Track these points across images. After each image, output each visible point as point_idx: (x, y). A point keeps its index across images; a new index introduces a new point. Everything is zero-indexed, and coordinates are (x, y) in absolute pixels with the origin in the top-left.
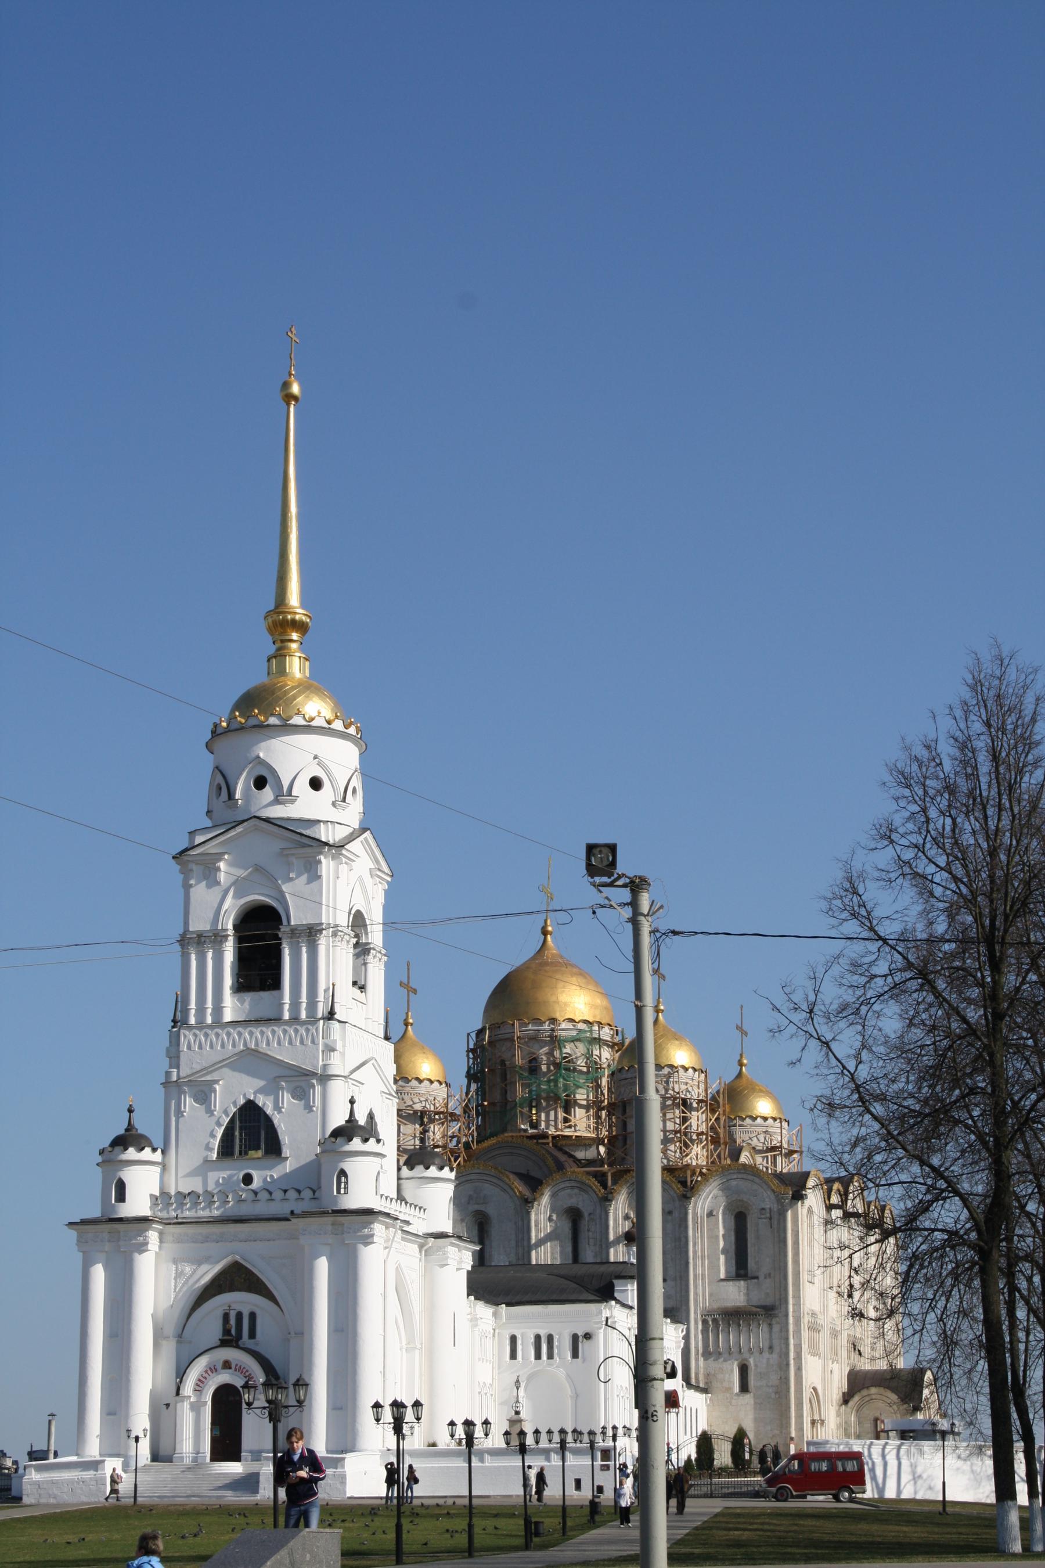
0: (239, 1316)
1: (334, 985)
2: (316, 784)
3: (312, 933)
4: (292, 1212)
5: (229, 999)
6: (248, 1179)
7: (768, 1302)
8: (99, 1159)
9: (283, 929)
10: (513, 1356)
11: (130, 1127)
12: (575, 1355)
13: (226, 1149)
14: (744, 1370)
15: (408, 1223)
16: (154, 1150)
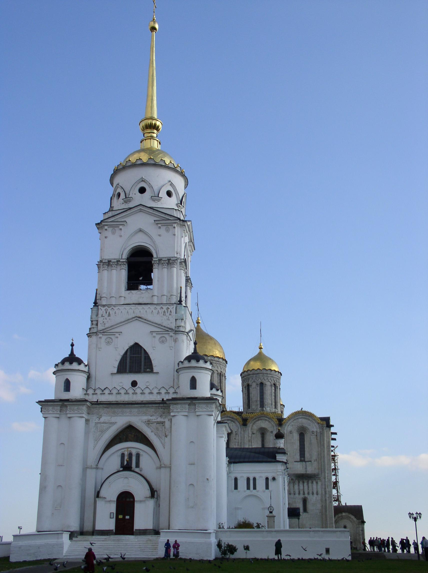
0: (130, 455)
1: (181, 288)
2: (169, 194)
3: (170, 262)
4: (163, 399)
6: (134, 384)
7: (316, 472)
10: (236, 487)
12: (267, 487)
13: (123, 368)
14: (305, 501)
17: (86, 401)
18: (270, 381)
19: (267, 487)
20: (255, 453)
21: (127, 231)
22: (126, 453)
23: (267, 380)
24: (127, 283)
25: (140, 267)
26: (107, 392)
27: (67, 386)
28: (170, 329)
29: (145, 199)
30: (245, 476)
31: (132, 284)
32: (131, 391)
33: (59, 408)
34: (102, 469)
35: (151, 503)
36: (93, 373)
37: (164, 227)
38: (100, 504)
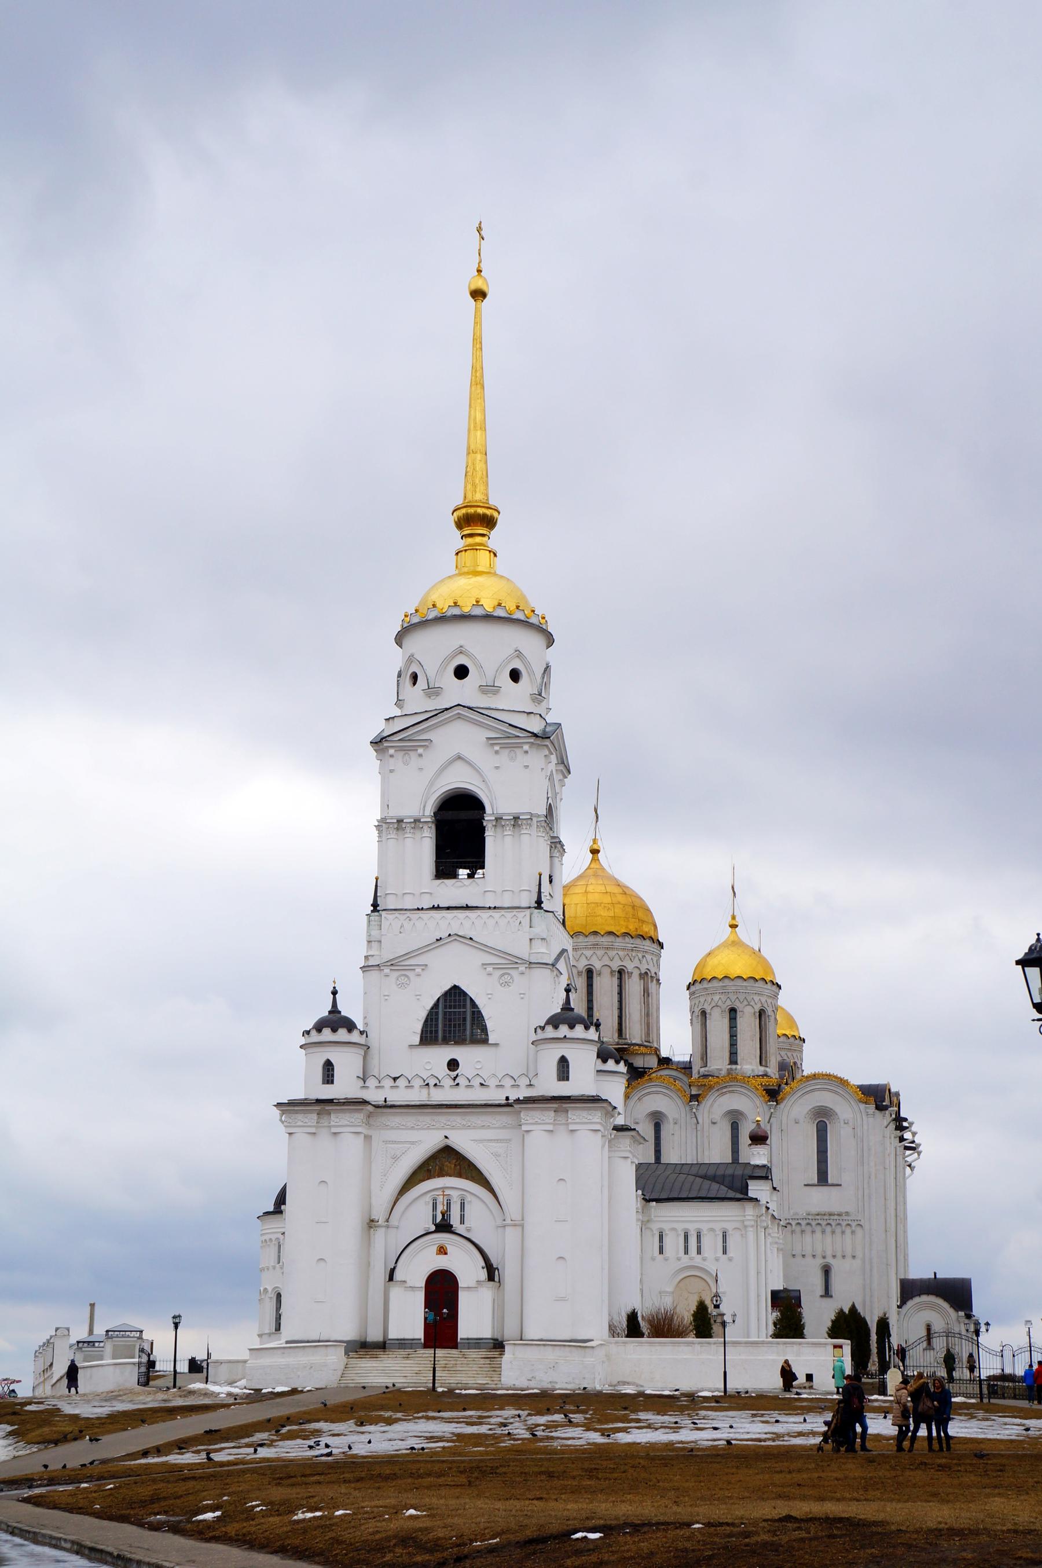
1: (540, 875)
2: (515, 676)
4: (507, 1098)
6: (453, 1065)
8: (303, 1041)
11: (334, 1010)
14: (827, 1271)
17: (365, 1102)
18: (752, 1003)
19: (725, 1252)
20: (705, 1177)
22: (440, 1199)
23: (745, 1003)
24: (436, 862)
25: (459, 833)
27: (328, 1072)
30: (681, 1227)
31: (444, 870)
33: (315, 1116)
34: (397, 1228)
35: (487, 1293)
37: (507, 751)
38: (396, 1293)
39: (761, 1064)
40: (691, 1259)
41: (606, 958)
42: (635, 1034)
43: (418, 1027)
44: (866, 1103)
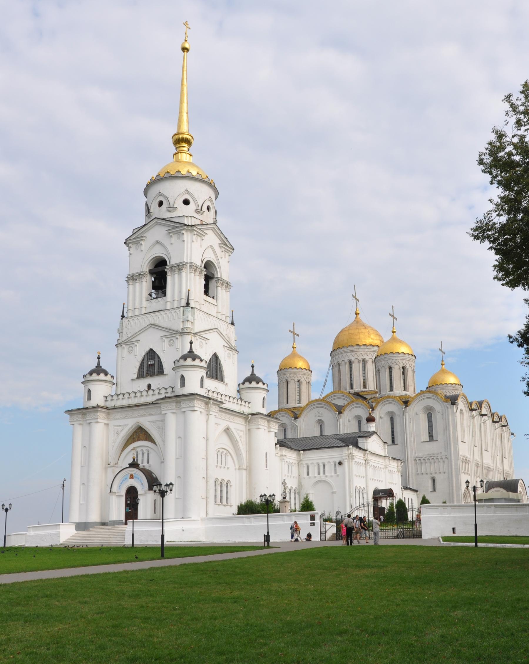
2: (186, 202)
3: (180, 267)
5: (145, 304)
6: (149, 386)
9: (167, 267)
11: (99, 366)
14: (434, 481)
15: (222, 403)
16: (106, 374)
18: (398, 364)
19: (336, 472)
20: (338, 439)
21: (145, 245)
26: (121, 397)
28: (175, 331)
29: (163, 212)
30: (315, 462)
32: (138, 394)
33: (81, 416)
36: (119, 381)
39: (405, 390)
40: (321, 477)
41: (356, 355)
42: (371, 386)
43: (136, 370)
44: (446, 402)
